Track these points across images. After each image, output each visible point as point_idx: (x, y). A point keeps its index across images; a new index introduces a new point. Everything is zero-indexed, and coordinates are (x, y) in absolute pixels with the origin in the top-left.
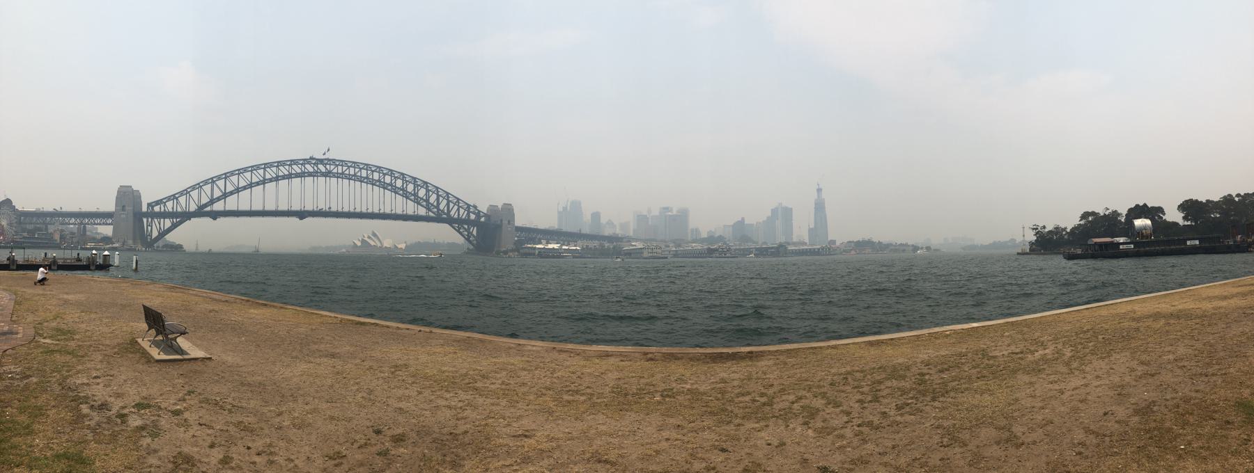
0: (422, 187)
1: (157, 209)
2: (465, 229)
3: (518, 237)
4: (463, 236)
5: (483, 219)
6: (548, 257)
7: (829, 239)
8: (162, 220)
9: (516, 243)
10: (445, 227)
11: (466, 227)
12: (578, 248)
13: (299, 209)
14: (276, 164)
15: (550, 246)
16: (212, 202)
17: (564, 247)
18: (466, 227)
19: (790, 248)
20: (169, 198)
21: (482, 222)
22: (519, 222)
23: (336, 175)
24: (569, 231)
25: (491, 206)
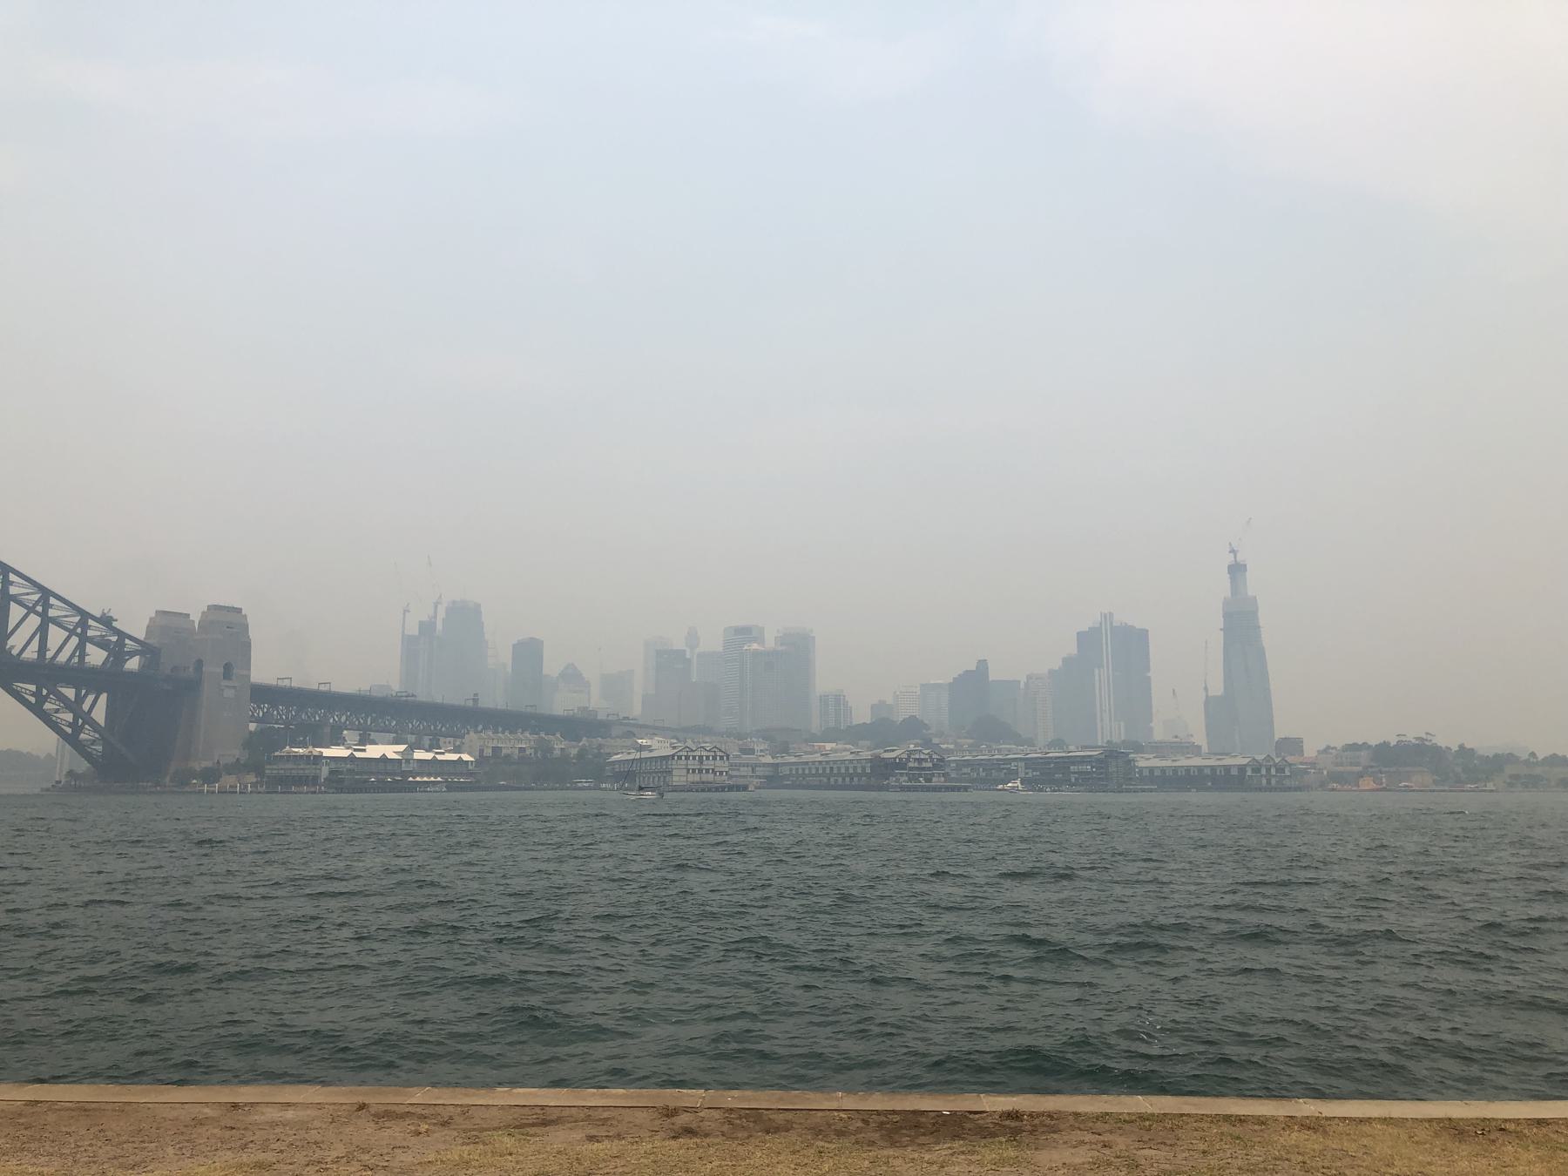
2: (62, 698)
3: (258, 720)
4: (54, 726)
6: (360, 787)
7: (1276, 739)
9: (250, 742)
11: (70, 693)
12: (466, 757)
15: (373, 751)
17: (419, 755)
18: (70, 693)
19: (1144, 762)
21: (131, 673)
22: (265, 669)
24: (439, 700)
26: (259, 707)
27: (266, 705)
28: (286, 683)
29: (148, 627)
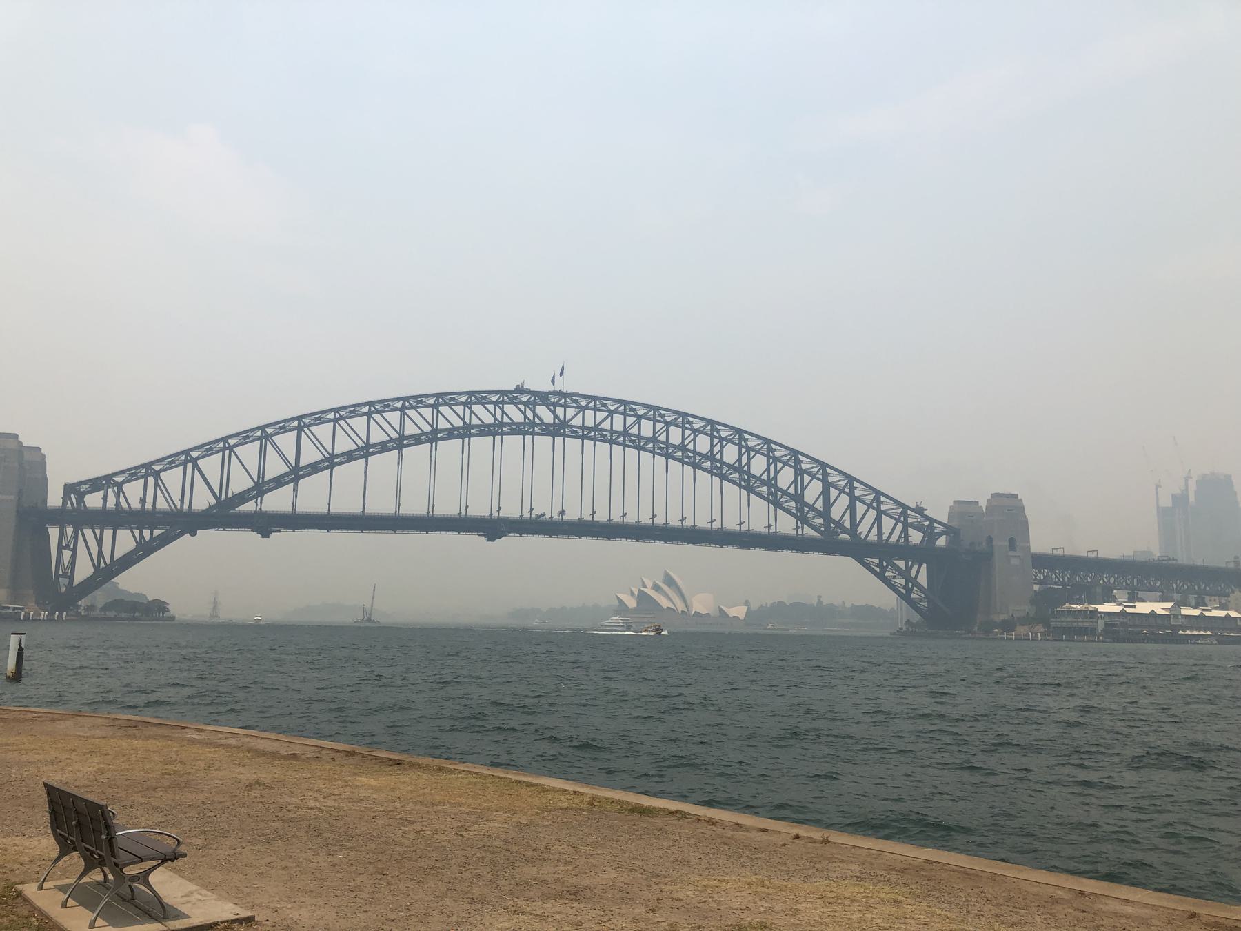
0: (785, 463)
1: (93, 501)
2: (896, 568)
3: (1040, 583)
4: (894, 588)
5: (942, 541)
8: (108, 533)
9: (1037, 599)
10: (847, 564)
11: (901, 564)
13: (486, 514)
14: (432, 401)
16: (260, 488)
18: (901, 564)
20: (132, 474)
21: (941, 549)
22: (1041, 541)
23: (580, 431)
25: (954, 502)
26: (1040, 572)
27: (1046, 570)
28: (1060, 552)
29: (949, 513)
